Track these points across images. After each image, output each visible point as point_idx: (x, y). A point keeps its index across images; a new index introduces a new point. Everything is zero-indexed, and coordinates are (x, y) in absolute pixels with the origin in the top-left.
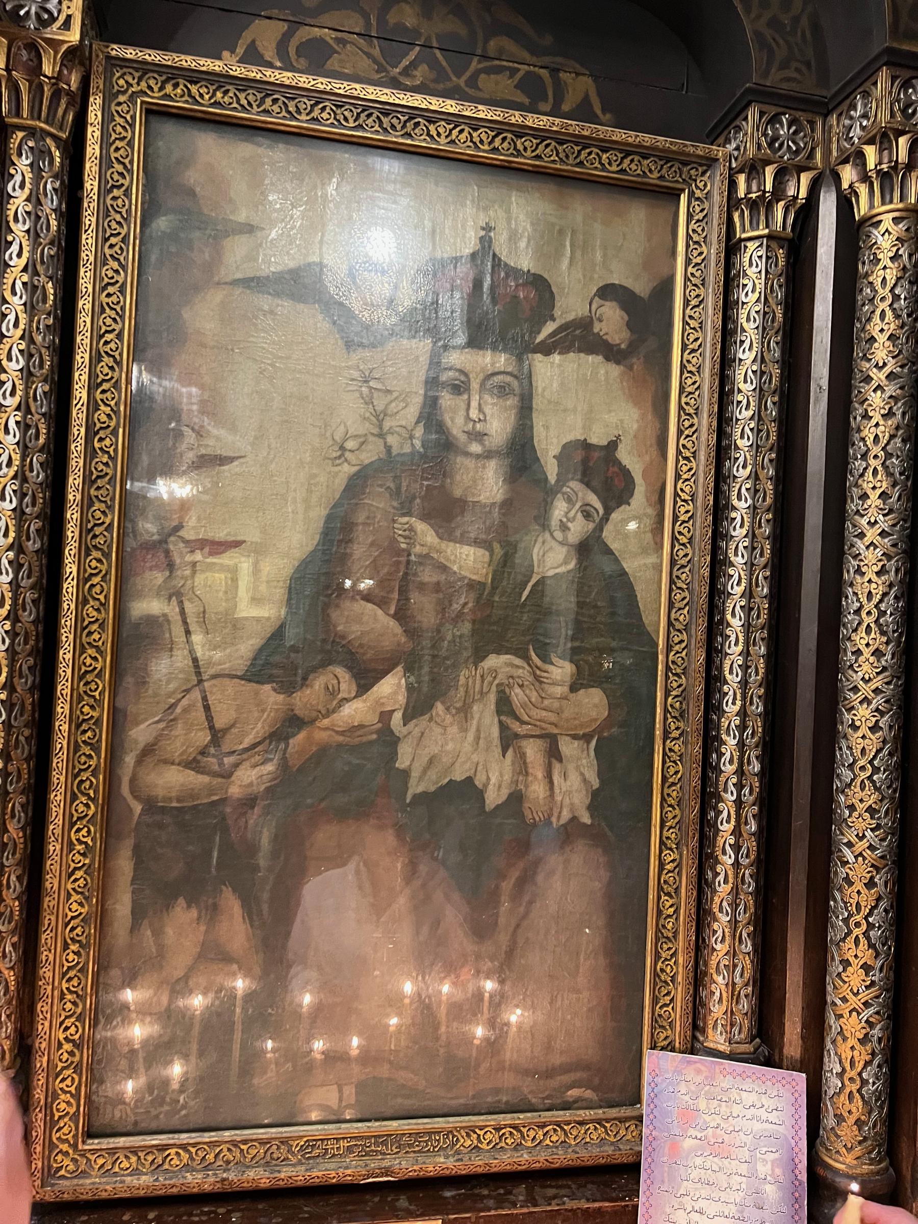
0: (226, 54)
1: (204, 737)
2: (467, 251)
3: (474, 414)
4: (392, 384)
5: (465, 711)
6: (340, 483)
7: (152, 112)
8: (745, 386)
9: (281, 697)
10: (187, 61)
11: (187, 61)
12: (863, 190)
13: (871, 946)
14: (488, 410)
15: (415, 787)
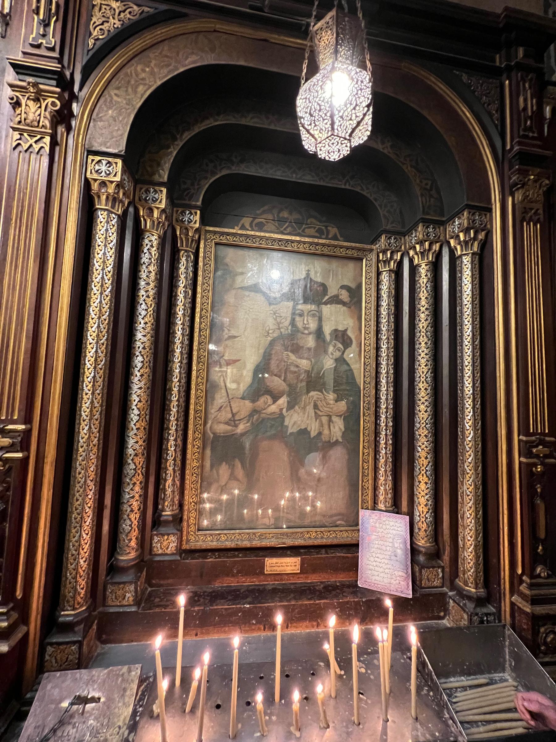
0: (236, 227)
1: (230, 416)
2: (303, 277)
3: (305, 322)
4: (282, 315)
5: (304, 408)
6: (268, 342)
7: (216, 244)
8: (384, 312)
9: (251, 404)
10: (226, 230)
11: (226, 230)
12: (416, 257)
13: (427, 476)
14: (310, 321)
15: (290, 431)
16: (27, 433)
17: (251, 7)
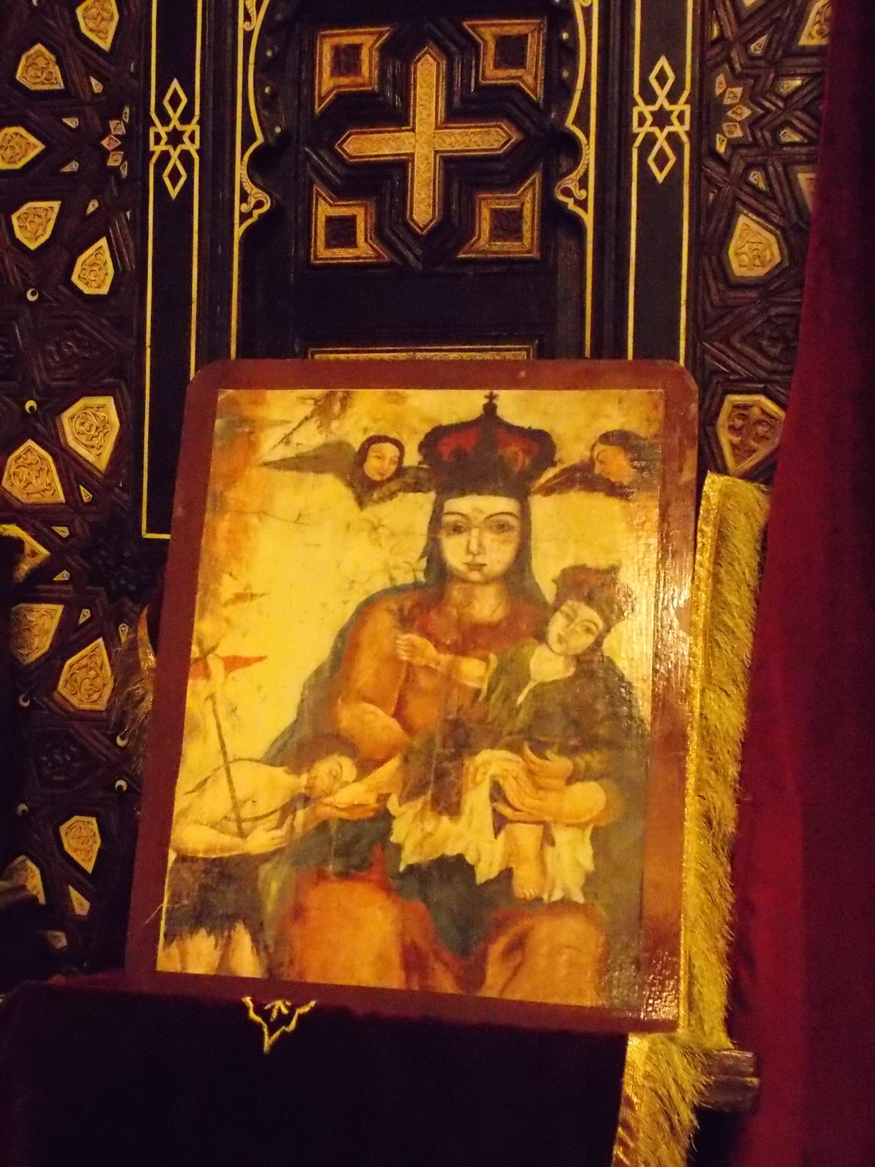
15: (409, 857)
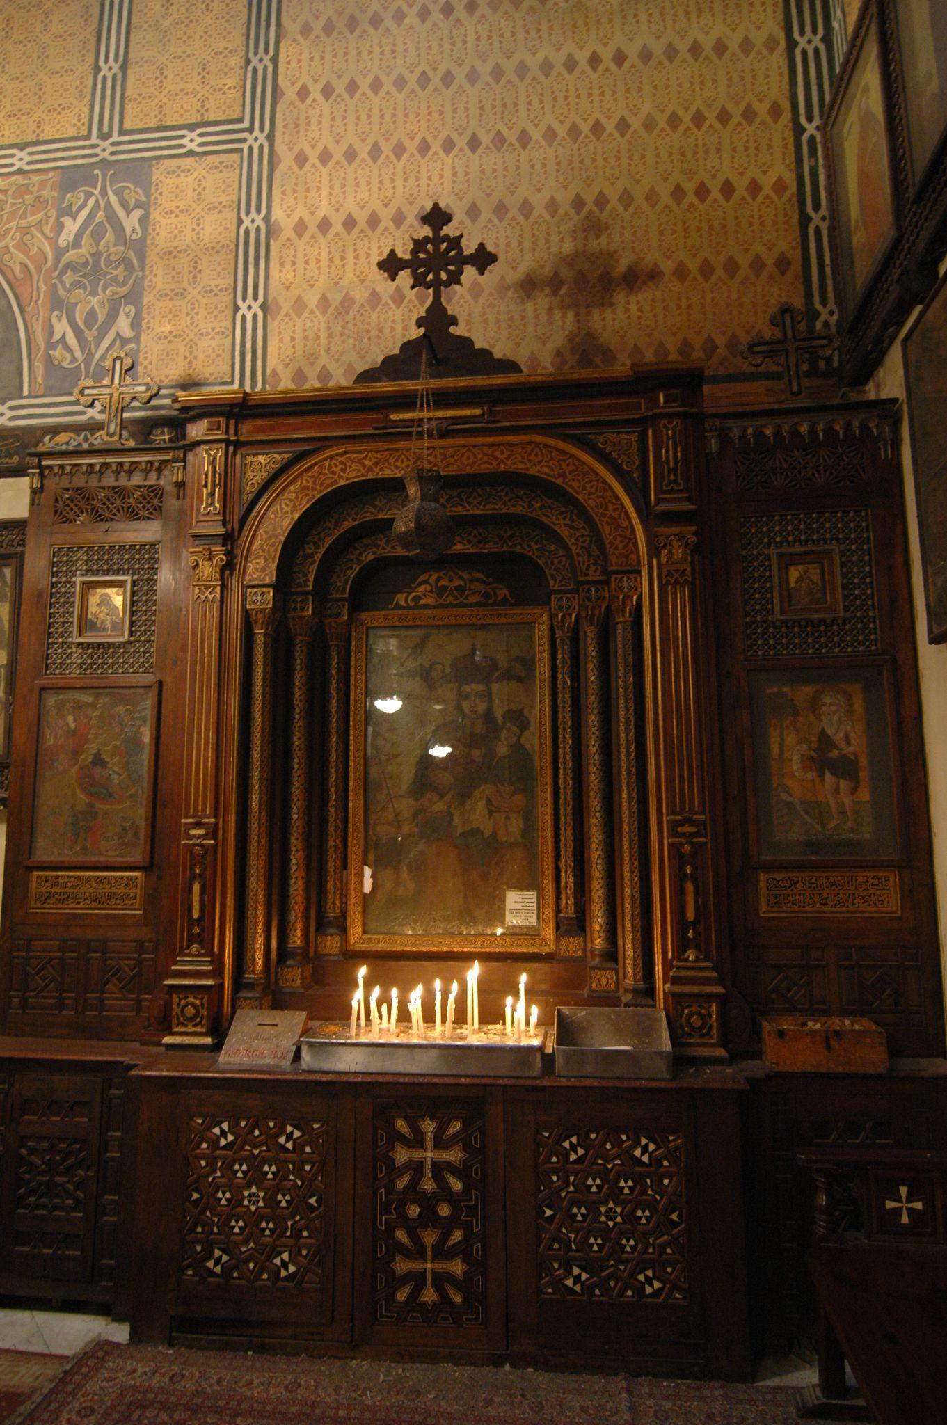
16: (216, 824)
17: (376, 428)
